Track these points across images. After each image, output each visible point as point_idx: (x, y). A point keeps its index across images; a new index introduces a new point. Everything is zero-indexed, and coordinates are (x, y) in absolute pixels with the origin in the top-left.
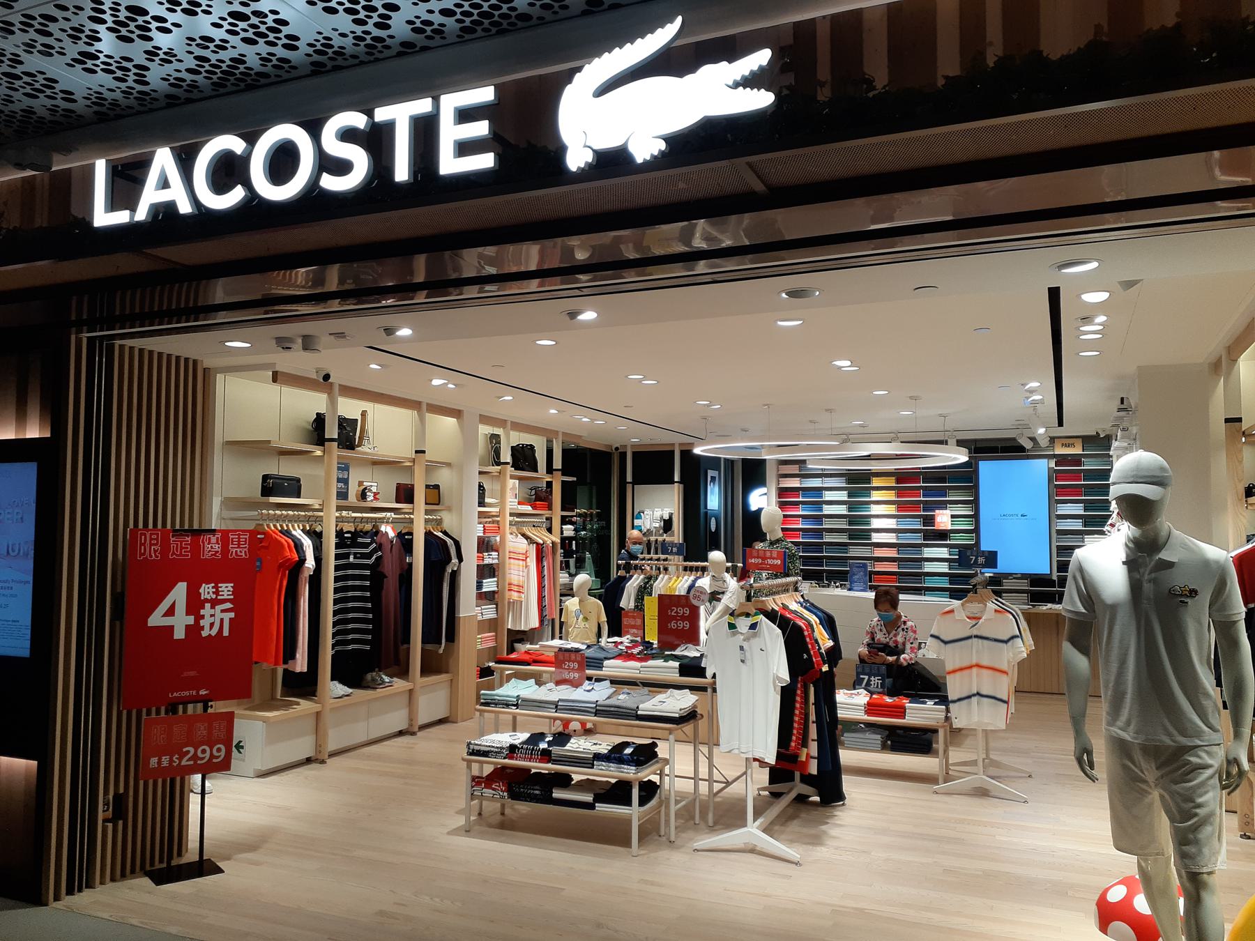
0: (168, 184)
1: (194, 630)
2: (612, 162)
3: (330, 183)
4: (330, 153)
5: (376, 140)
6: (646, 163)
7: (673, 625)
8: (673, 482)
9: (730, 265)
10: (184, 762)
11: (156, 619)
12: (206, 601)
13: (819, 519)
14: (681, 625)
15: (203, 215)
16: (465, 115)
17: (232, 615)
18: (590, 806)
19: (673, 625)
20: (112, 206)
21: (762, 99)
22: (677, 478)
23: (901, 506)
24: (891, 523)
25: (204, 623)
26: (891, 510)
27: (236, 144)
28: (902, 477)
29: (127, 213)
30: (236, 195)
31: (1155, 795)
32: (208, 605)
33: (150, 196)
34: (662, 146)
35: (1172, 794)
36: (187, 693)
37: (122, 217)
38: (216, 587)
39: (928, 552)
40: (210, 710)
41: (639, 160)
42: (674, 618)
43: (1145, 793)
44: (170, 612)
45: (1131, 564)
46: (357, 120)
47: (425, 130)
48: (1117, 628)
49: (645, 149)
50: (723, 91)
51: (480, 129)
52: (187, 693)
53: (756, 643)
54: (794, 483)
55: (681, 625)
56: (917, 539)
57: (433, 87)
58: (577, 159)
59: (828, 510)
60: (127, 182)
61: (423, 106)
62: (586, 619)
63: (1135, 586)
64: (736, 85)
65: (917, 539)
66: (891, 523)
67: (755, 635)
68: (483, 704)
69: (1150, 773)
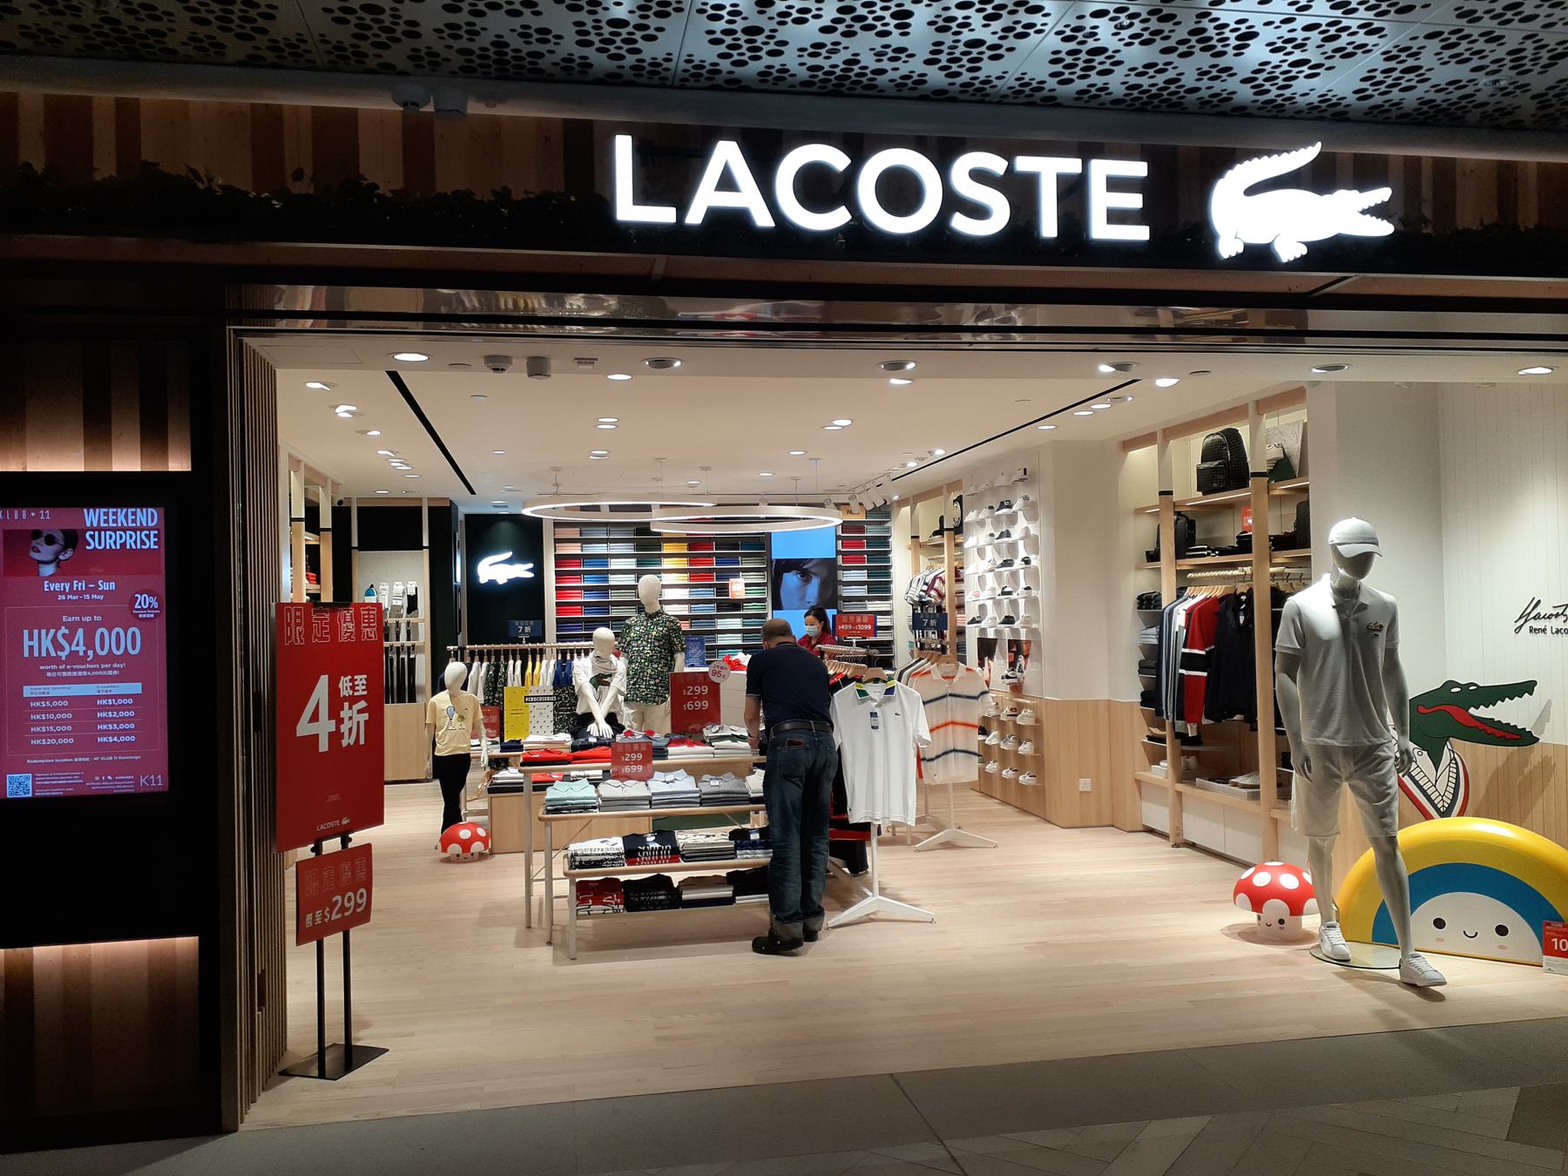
0: (725, 182)
1: (335, 737)
2: (1258, 257)
3: (961, 224)
4: (971, 191)
5: (1021, 190)
6: (1289, 263)
7: (689, 706)
8: (421, 548)
9: (1039, 337)
10: (334, 917)
11: (304, 728)
12: (345, 698)
13: (605, 590)
14: (698, 704)
15: (785, 234)
16: (1115, 184)
17: (366, 716)
18: (729, 901)
19: (689, 706)
20: (643, 195)
21: (1384, 228)
22: (426, 543)
23: (693, 574)
24: (683, 594)
25: (344, 729)
26: (683, 579)
27: (838, 160)
28: (694, 543)
29: (672, 211)
30: (839, 217)
31: (1345, 785)
32: (346, 705)
33: (706, 199)
34: (1304, 251)
35: (1369, 782)
36: (331, 824)
37: (665, 215)
38: (352, 680)
39: (722, 624)
40: (350, 845)
41: (1284, 260)
42: (690, 698)
43: (1338, 786)
44: (315, 718)
45: (1339, 608)
46: (997, 165)
47: (1073, 192)
48: (1331, 660)
49: (1289, 251)
50: (1351, 214)
51: (1134, 201)
52: (331, 824)
53: (891, 708)
54: (575, 549)
55: (698, 704)
56: (711, 610)
57: (1087, 152)
58: (1228, 247)
59: (614, 580)
60: (668, 173)
61: (1073, 166)
62: (462, 718)
63: (1344, 624)
64: (1364, 212)
65: (711, 610)
66: (683, 594)
67: (889, 700)
68: (549, 812)
69: (1345, 767)
